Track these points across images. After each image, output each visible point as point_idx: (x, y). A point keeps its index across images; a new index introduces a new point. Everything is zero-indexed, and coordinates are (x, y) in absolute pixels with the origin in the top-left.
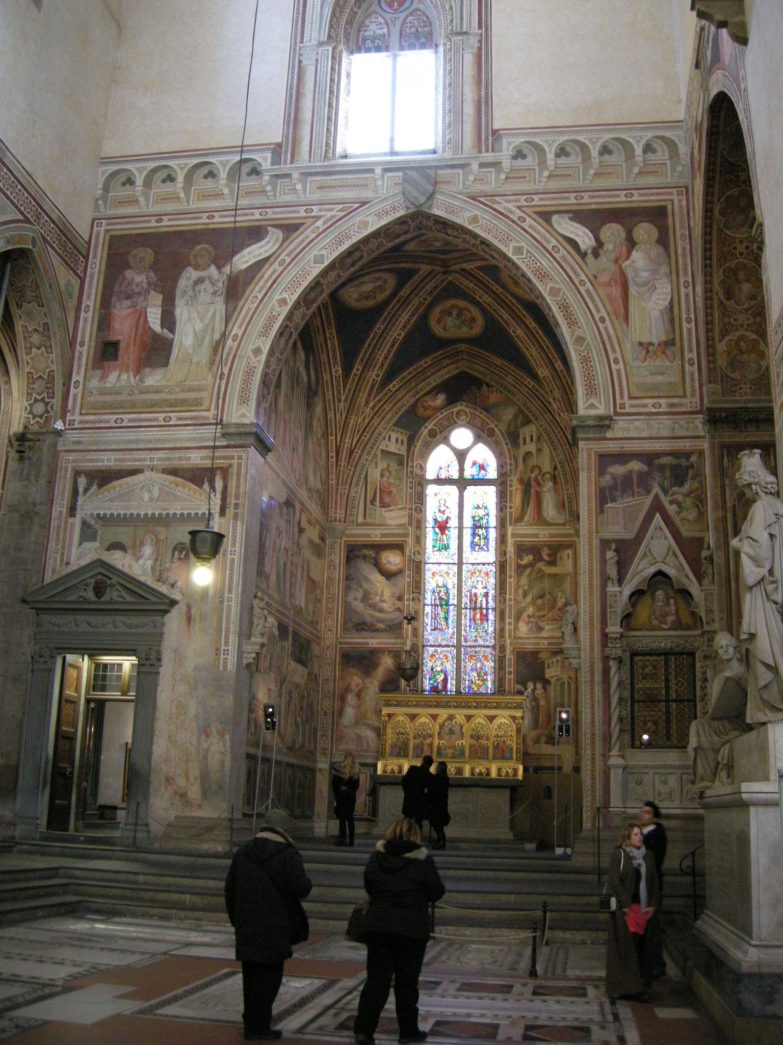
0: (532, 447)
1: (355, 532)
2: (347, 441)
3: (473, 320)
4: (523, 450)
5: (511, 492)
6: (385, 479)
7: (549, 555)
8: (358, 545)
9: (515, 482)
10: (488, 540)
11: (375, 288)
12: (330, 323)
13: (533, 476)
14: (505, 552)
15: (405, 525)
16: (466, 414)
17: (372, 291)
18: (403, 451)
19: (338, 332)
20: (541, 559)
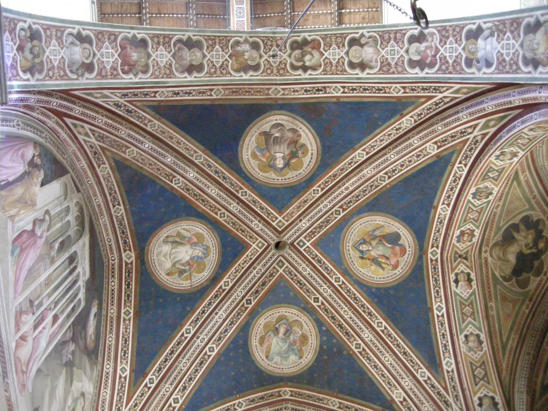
3: (304, 339)
11: (192, 258)
12: (129, 296)
17: (188, 263)
19: (137, 314)
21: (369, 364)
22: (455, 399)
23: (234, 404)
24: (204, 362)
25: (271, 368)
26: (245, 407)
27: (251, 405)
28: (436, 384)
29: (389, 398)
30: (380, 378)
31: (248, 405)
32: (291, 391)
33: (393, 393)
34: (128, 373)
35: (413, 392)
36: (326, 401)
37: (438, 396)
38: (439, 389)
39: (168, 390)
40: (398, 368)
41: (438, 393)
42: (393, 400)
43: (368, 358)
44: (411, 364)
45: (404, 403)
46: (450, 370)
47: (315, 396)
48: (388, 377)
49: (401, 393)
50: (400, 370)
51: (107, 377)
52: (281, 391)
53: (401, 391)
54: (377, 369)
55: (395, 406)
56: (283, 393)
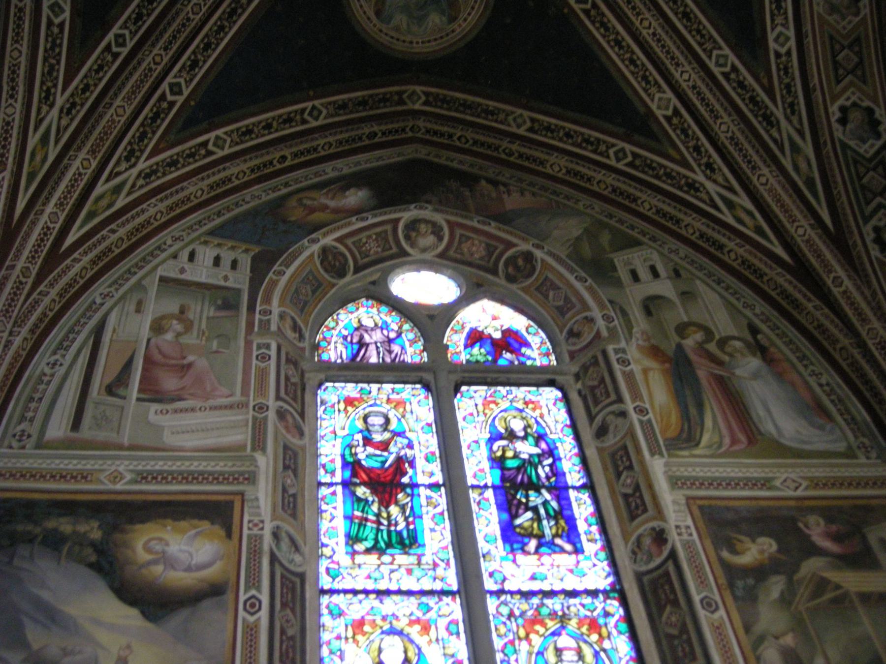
0: (665, 288)
1: (28, 464)
2: (50, 208)
4: (634, 295)
5: (630, 377)
6: (169, 336)
7: (837, 538)
8: (30, 505)
9: (633, 353)
10: (571, 522)
13: (689, 343)
14: (660, 537)
15: (242, 447)
16: (437, 231)
18: (240, 280)
20: (812, 550)
21: (604, 36)
22: (788, 111)
23: (303, 111)
24: (240, 11)
25: (385, 39)
26: (325, 118)
27: (337, 115)
28: (750, 80)
29: (642, 110)
30: (627, 66)
31: (332, 116)
32: (427, 94)
33: (652, 100)
34: (67, 14)
35: (699, 93)
36: (502, 116)
37: (751, 106)
38: (753, 90)
39: (158, 59)
40: (669, 43)
41: (753, 99)
42: (650, 113)
43: (603, 24)
44: (698, 38)
45: (675, 121)
46: (783, 50)
47: (480, 105)
48: (643, 65)
49: (669, 100)
50: (673, 48)
51: (20, 18)
52: (405, 92)
53: (669, 94)
54: (621, 47)
55: (655, 128)
56: (409, 97)
